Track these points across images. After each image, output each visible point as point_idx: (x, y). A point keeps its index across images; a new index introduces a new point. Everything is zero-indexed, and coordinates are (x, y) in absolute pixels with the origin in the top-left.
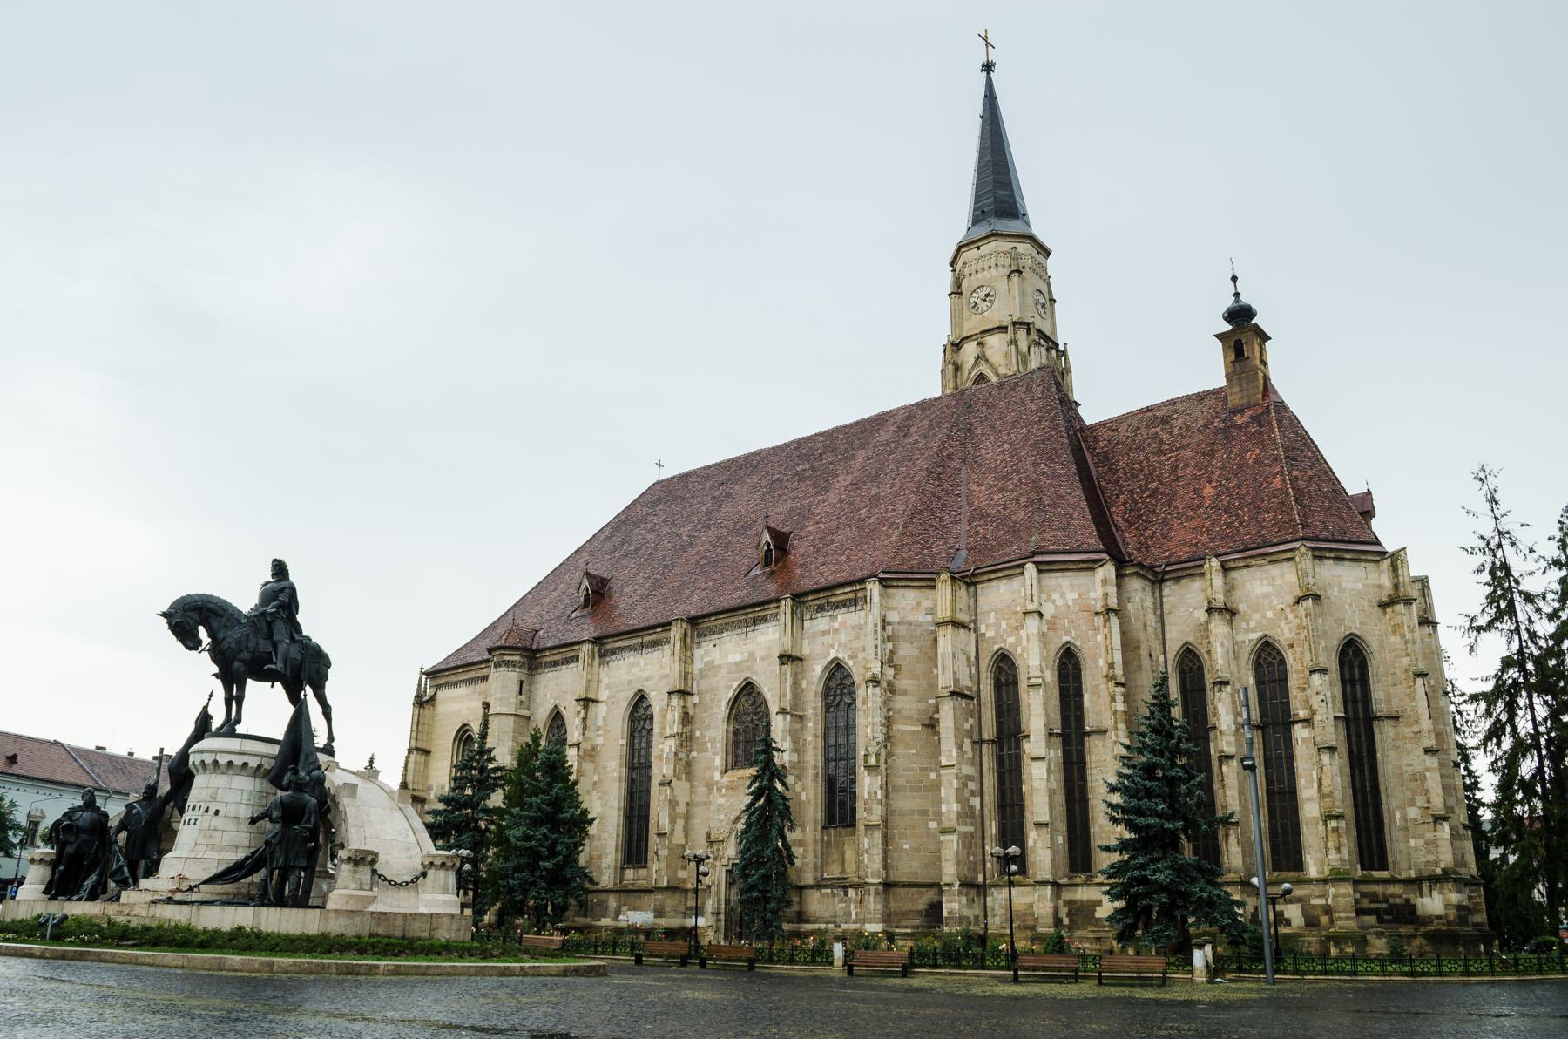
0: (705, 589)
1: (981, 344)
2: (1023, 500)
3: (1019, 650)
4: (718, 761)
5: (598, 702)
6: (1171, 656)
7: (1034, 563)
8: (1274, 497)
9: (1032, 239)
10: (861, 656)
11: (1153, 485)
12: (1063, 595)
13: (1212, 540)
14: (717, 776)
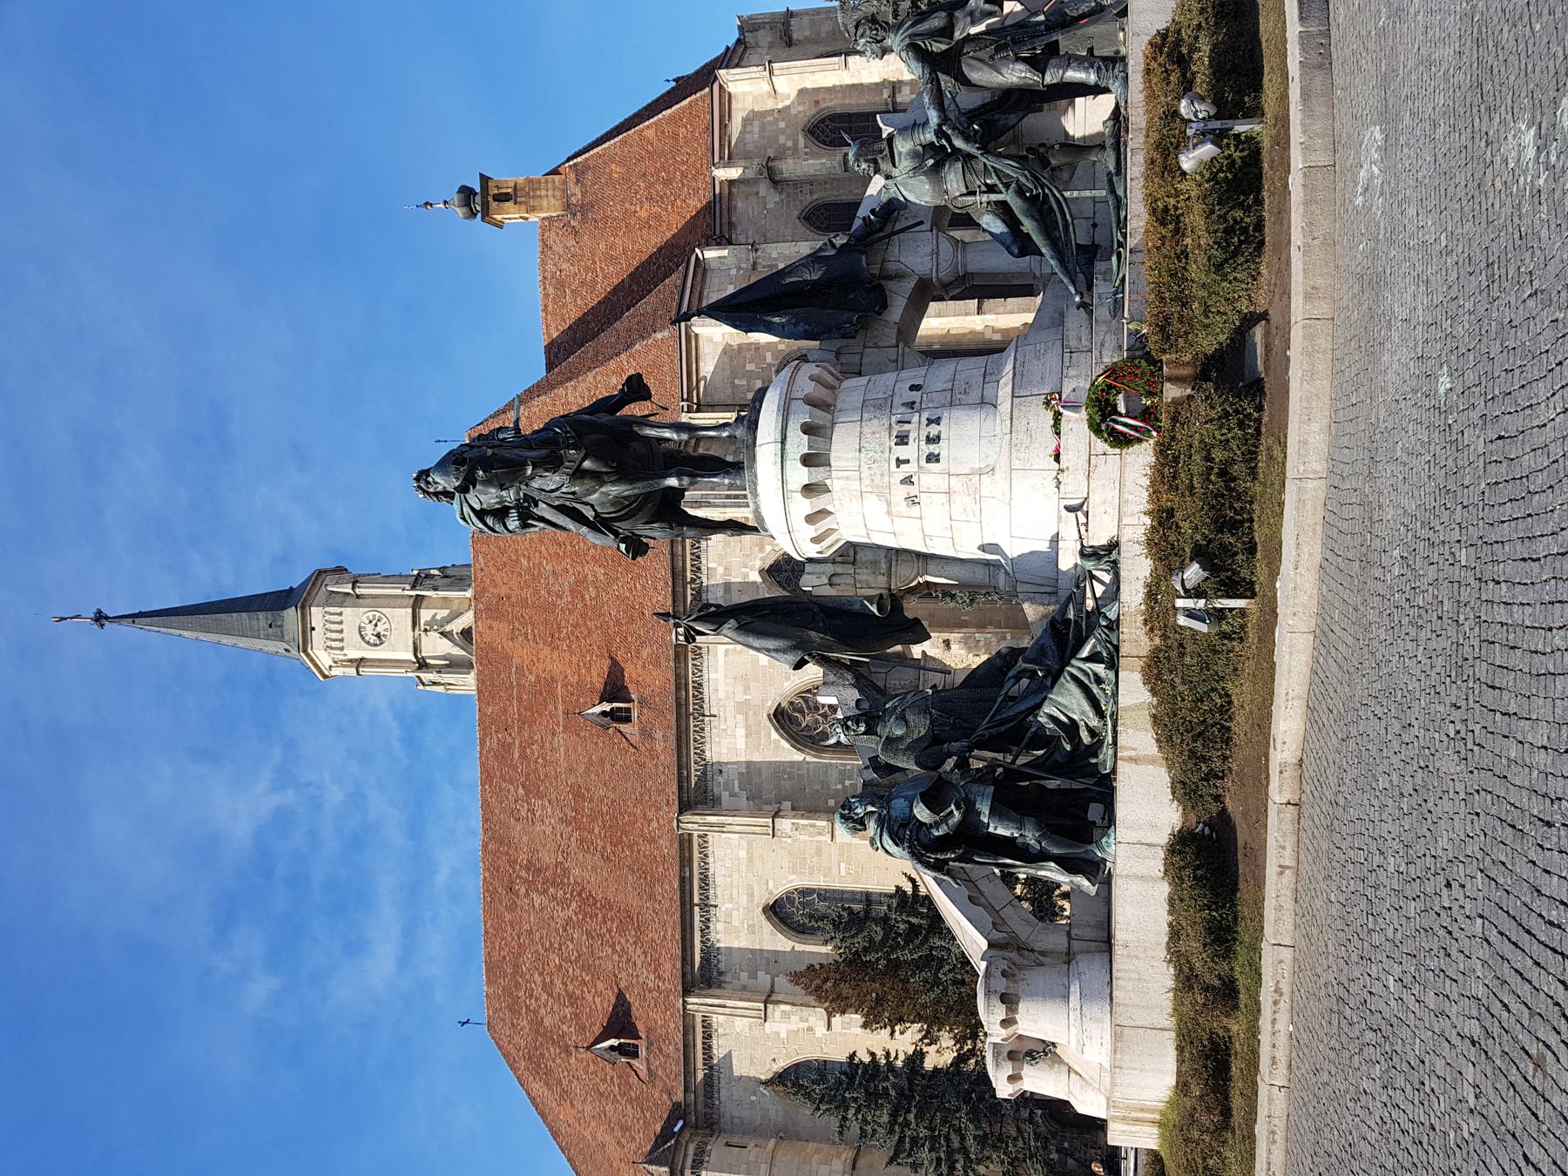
0: (645, 815)
5: (772, 992)
8: (663, 133)
13: (696, 191)
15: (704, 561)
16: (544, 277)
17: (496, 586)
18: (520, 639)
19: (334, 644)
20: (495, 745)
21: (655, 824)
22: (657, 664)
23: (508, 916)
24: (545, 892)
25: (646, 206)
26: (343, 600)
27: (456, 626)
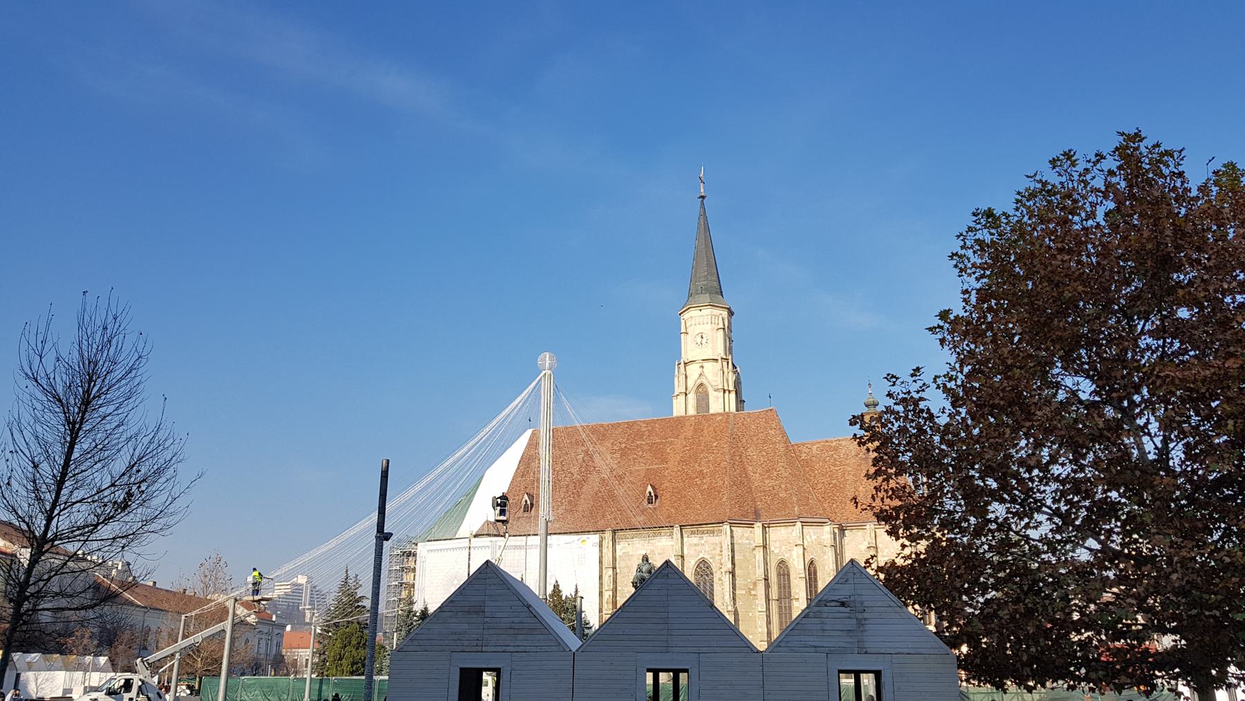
2: (783, 486)
3: (791, 560)
7: (801, 522)
10: (718, 558)
11: (834, 482)
12: (811, 537)
15: (706, 535)
16: (839, 440)
18: (684, 443)
20: (643, 429)
21: (609, 517)
22: (669, 517)
23: (573, 440)
25: (864, 490)
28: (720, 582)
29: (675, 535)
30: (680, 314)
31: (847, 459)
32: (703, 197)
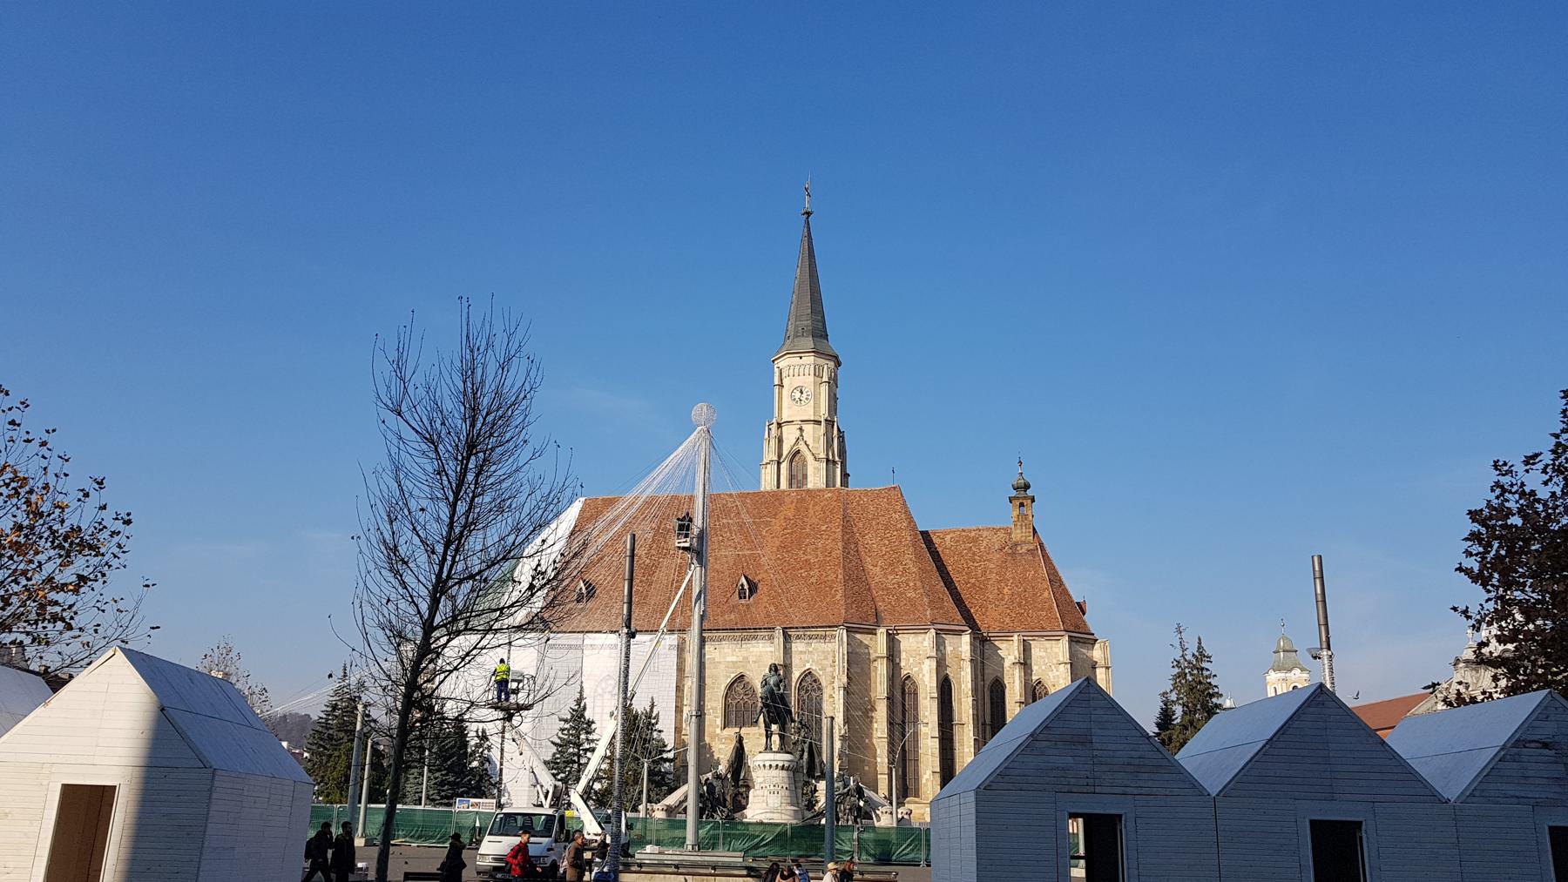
1: (801, 429)
2: (912, 584)
3: (921, 675)
4: (719, 721)
6: (988, 683)
9: (836, 357)
14: (718, 731)
15: (815, 641)
17: (813, 506)
19: (791, 371)
24: (653, 541)
25: (1010, 592)
26: (817, 375)
27: (802, 447)
28: (832, 700)
29: (776, 640)
30: (773, 361)
31: (988, 554)
32: (808, 214)
